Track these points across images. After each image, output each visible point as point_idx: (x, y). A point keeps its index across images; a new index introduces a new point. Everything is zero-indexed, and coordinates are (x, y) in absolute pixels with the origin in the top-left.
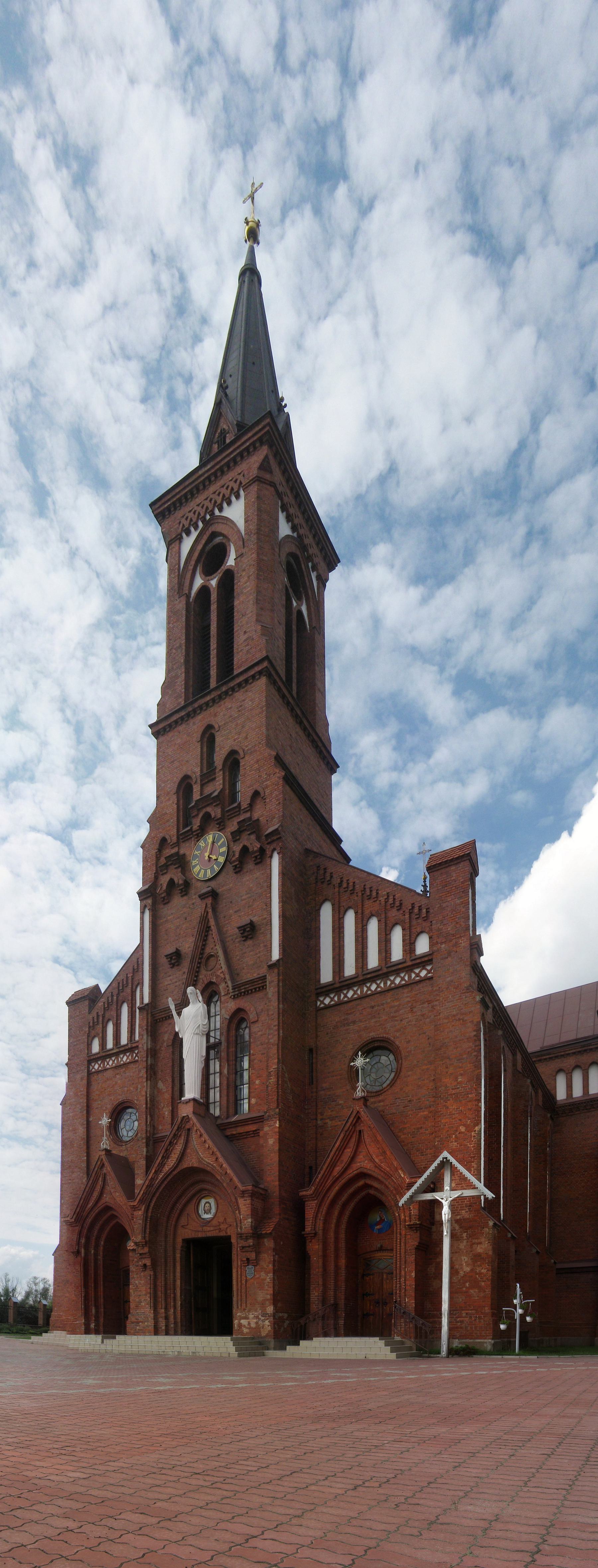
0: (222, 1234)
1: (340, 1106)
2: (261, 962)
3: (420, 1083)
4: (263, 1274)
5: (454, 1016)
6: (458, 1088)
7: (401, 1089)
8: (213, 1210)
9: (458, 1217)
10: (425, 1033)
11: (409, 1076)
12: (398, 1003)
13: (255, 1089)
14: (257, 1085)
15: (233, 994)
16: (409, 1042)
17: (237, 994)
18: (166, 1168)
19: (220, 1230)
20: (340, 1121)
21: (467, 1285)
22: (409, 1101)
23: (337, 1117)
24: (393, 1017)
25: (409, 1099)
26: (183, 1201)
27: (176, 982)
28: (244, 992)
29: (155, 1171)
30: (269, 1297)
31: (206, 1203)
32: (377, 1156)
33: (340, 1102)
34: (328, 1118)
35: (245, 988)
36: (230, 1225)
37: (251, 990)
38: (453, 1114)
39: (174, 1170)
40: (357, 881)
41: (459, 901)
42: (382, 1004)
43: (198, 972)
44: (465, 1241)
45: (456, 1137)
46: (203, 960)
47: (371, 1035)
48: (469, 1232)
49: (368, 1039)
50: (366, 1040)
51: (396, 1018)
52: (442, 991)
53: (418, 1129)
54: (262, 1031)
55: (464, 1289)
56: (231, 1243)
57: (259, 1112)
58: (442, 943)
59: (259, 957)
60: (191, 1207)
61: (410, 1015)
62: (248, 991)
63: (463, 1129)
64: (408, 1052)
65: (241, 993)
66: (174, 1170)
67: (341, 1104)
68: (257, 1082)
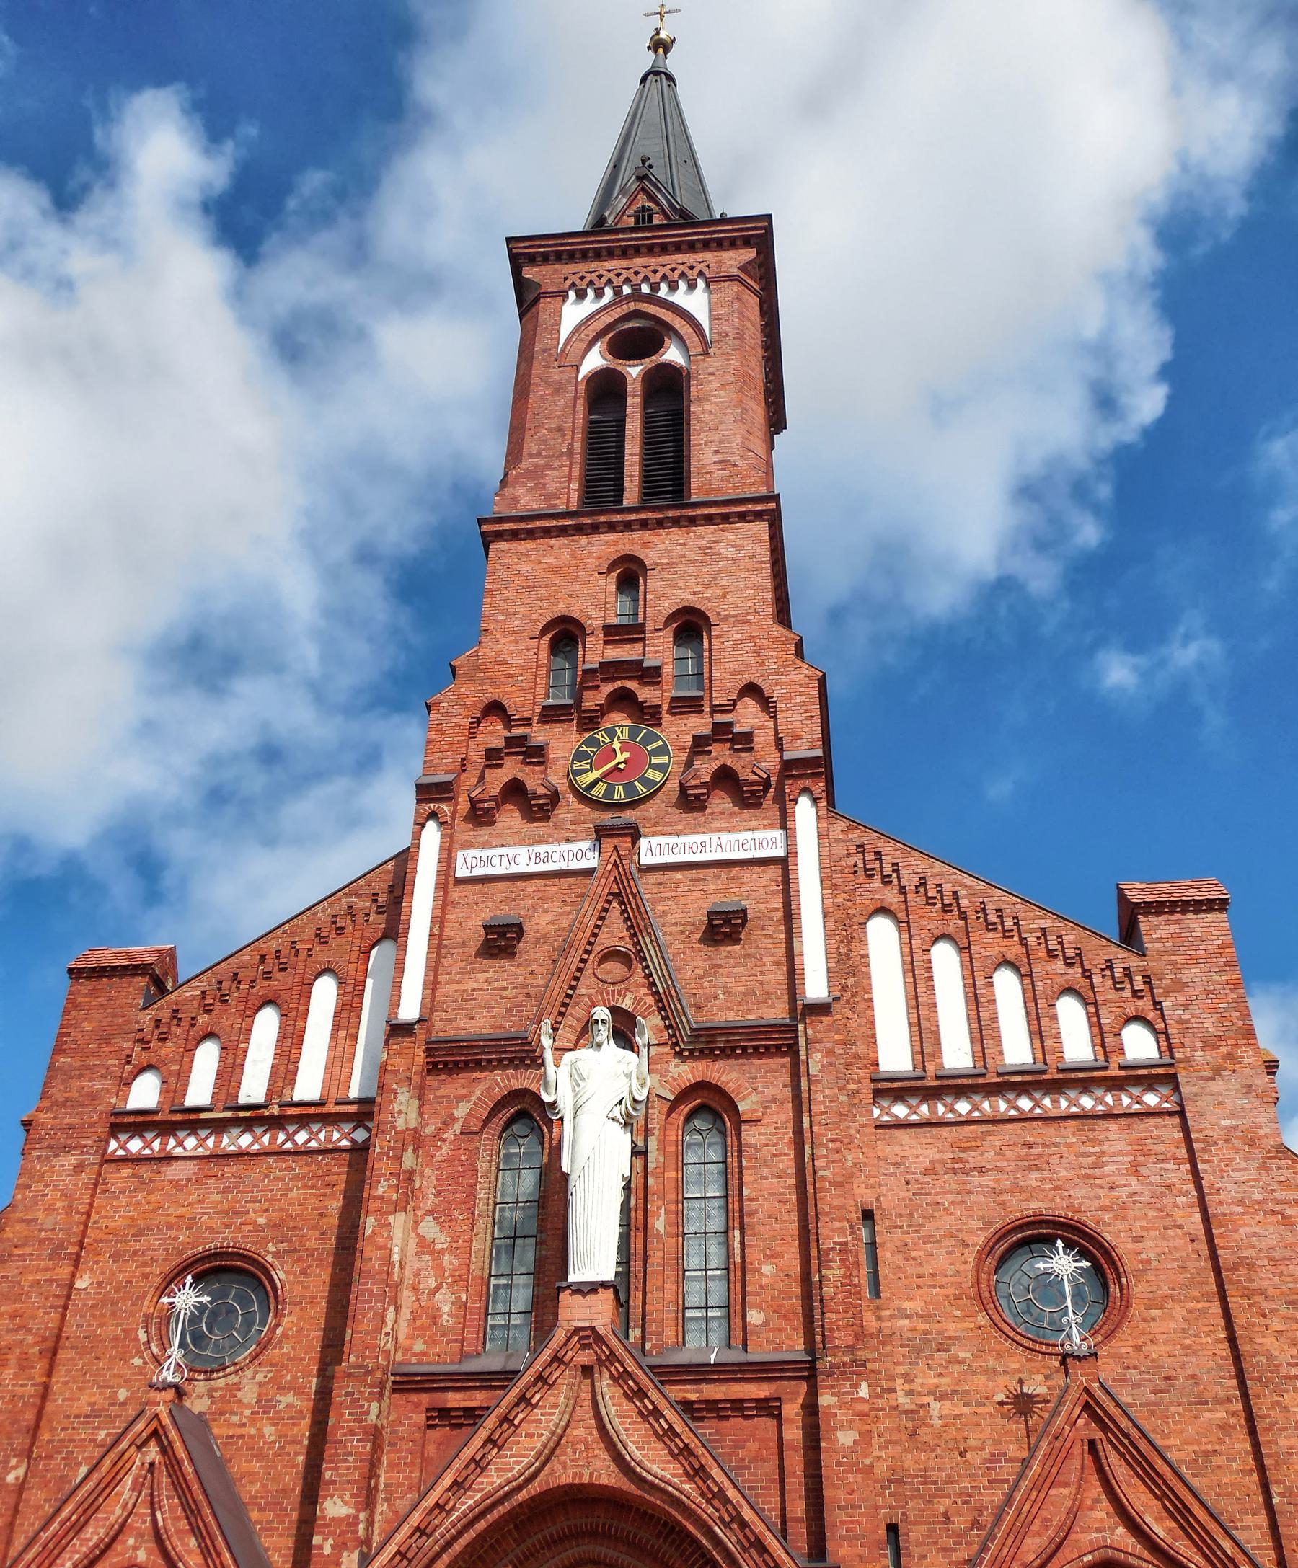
1: (963, 1367)
2: (768, 993)
3: (1188, 1342)
7: (1138, 1349)
10: (1180, 1227)
11: (1153, 1319)
12: (1096, 1149)
13: (761, 1287)
14: (767, 1276)
16: (1138, 1239)
17: (701, 1051)
18: (493, 1480)
20: (966, 1405)
22: (1168, 1378)
23: (956, 1392)
24: (1088, 1176)
25: (1164, 1372)
27: (505, 989)
28: (722, 1050)
29: (455, 1483)
33: (962, 1355)
34: (930, 1393)
35: (727, 1041)
39: (519, 1488)
40: (962, 892)
41: (1218, 978)
42: (1056, 1145)
43: (577, 979)
47: (1032, 1205)
49: (1025, 1213)
50: (1018, 1215)
51: (1097, 1181)
52: (1216, 1144)
53: (1206, 1453)
54: (776, 1145)
57: (776, 1349)
58: (1194, 1048)
59: (761, 983)
61: (1133, 1180)
62: (733, 1049)
64: (1141, 1262)
65: (712, 1050)
66: (519, 1488)
67: (964, 1361)
68: (767, 1269)
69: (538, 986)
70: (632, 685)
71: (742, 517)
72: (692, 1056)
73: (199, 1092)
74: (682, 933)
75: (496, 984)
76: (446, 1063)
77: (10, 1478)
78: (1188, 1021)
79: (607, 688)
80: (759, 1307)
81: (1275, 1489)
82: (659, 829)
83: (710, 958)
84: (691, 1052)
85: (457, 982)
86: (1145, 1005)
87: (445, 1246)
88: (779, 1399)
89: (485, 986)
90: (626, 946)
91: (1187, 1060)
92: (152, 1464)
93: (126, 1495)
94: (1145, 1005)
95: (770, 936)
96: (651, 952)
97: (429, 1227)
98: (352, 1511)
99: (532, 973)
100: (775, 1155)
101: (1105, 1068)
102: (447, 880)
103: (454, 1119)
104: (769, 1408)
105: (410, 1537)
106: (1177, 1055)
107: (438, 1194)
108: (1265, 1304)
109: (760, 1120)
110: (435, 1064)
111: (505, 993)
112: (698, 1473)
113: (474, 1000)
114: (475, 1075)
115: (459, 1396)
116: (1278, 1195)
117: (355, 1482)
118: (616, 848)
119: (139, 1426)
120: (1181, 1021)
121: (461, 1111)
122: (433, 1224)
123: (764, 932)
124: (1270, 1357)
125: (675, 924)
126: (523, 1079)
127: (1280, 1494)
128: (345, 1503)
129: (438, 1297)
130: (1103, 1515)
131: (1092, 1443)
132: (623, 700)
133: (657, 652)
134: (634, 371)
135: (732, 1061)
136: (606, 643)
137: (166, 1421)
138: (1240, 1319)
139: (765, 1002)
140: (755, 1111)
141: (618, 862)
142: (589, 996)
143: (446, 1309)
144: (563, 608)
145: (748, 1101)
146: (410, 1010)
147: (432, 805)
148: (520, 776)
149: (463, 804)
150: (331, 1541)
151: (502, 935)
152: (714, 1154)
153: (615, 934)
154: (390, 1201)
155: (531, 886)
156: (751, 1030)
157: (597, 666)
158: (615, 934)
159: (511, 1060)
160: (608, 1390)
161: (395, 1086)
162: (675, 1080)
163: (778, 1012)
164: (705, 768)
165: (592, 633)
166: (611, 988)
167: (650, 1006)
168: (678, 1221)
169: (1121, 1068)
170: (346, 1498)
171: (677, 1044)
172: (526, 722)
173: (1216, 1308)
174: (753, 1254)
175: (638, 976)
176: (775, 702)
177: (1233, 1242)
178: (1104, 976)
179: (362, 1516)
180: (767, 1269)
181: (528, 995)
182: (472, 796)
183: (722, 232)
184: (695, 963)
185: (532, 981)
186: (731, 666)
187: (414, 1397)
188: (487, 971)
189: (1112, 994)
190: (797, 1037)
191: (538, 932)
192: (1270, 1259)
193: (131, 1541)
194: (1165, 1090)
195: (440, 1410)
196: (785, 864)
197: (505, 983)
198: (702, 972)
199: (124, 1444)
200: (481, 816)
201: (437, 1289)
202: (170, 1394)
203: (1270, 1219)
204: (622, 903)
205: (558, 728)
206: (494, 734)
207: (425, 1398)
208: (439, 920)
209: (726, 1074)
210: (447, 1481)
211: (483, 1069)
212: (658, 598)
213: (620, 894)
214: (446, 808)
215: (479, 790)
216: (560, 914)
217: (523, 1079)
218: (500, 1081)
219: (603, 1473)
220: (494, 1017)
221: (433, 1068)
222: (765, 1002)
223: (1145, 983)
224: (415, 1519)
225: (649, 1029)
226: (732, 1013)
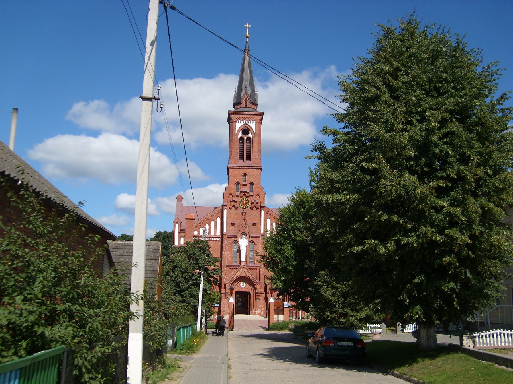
18: (237, 276)
70: (246, 193)
71: (258, 169)
73: (201, 233)
90: (245, 225)
97: (228, 252)
112: (252, 276)
121: (230, 242)
132: (244, 195)
134: (245, 137)
149: (228, 207)
153: (244, 224)
158: (244, 224)
160: (245, 269)
164: (253, 205)
183: (257, 113)
209: (254, 240)
218: (234, 239)
219: (245, 275)
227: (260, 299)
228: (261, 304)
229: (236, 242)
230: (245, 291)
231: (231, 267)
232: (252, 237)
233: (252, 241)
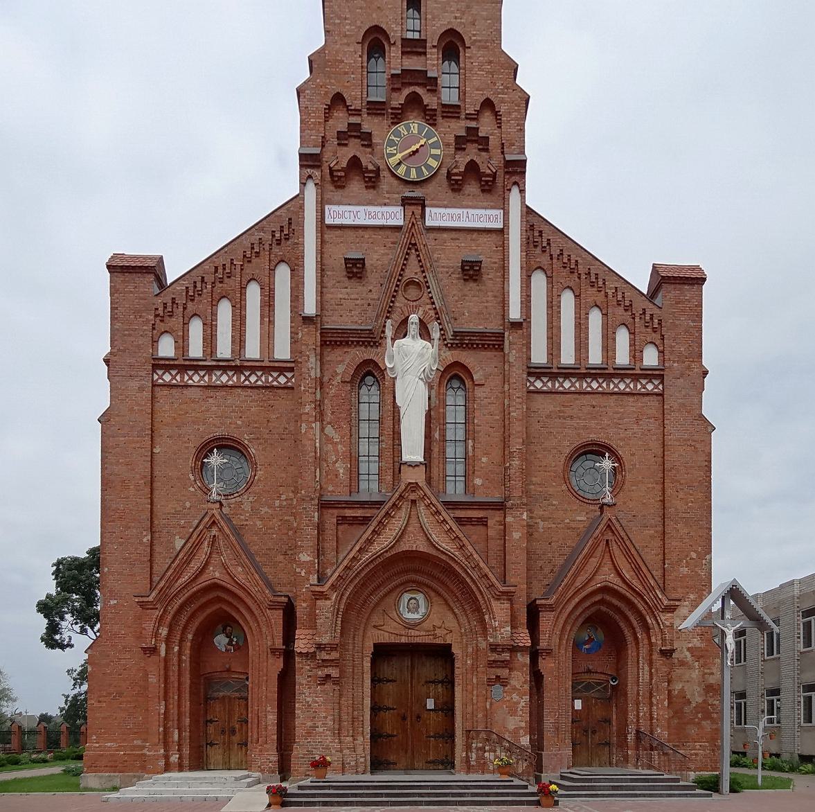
0: (438, 641)
2: (490, 314)
4: (515, 697)
5: (685, 440)
6: (689, 513)
8: (422, 610)
9: (690, 645)
13: (481, 468)
15: (452, 342)
19: (435, 636)
21: (700, 715)
26: (383, 591)
28: (467, 344)
30: (523, 724)
31: (411, 599)
32: (628, 572)
36: (451, 631)
37: (478, 345)
38: (685, 539)
41: (692, 324)
44: (697, 671)
45: (687, 561)
46: (402, 285)
48: (702, 661)
55: (696, 720)
56: (453, 654)
58: (674, 362)
60: (390, 600)
63: (694, 555)
68: (484, 459)
69: (374, 299)
72: (451, 347)
74: (447, 273)
75: (353, 297)
76: (330, 341)
77: (145, 540)
78: (674, 347)
79: (406, 92)
80: (480, 477)
81: (666, 562)
82: (435, 202)
83: (461, 290)
84: (452, 344)
85: (332, 293)
86: (657, 336)
87: (338, 440)
88: (487, 518)
89: (346, 297)
91: (670, 367)
92: (214, 536)
93: (206, 549)
94: (657, 336)
95: (491, 279)
96: (432, 283)
97: (329, 430)
98: (312, 559)
99: (371, 291)
100: (489, 403)
101: (634, 369)
102: (323, 228)
103: (337, 374)
104: (483, 522)
105: (343, 570)
106: (666, 365)
107: (333, 413)
108: (679, 487)
109: (483, 385)
110: (325, 341)
111: (358, 302)
113: (342, 305)
114: (345, 350)
115: (350, 511)
116: (695, 438)
117: (311, 546)
118: (413, 213)
119: (206, 519)
120: (671, 347)
121: (340, 369)
122: (331, 428)
123: (489, 277)
124: (676, 509)
125: (443, 267)
126: (369, 354)
127: (669, 564)
128: (309, 555)
129: (337, 465)
130: (607, 569)
131: (607, 541)
133: (434, 65)
135: (471, 352)
136: (403, 53)
137: (218, 517)
138: (668, 492)
139: (487, 319)
140: (482, 380)
141: (415, 222)
142: (401, 308)
143: (341, 471)
144: (375, 19)
145: (478, 374)
146: (310, 308)
147: (309, 170)
148: (358, 154)
150: (304, 570)
151: (354, 265)
152: (461, 401)
154: (312, 416)
155: (367, 235)
156: (482, 335)
157: (400, 72)
159: (363, 342)
161: (307, 353)
162: (444, 360)
163: (493, 326)
165: (395, 43)
166: (411, 304)
167: (432, 316)
168: (443, 435)
169: (642, 369)
170: (309, 553)
171: (445, 340)
172: (357, 112)
173: (659, 487)
174: (478, 452)
175: (425, 299)
176: (501, 115)
177: (672, 458)
178: (640, 318)
179: (316, 561)
180: (484, 459)
181: (369, 305)
182: (332, 166)
184: (454, 293)
185: (370, 296)
186: (477, 84)
187: (330, 511)
188: (346, 288)
189: (643, 329)
190: (503, 341)
191: (372, 265)
192: (685, 467)
193: (211, 568)
194: (656, 382)
195: (342, 517)
196: (502, 232)
197: (357, 296)
198: (457, 298)
199: (201, 527)
200: (336, 181)
201: (336, 462)
202: (218, 505)
203: (689, 448)
204: (417, 250)
205: (376, 120)
206: (341, 121)
207: (336, 512)
208: (321, 252)
209: (467, 358)
210: (357, 548)
211: (349, 346)
212: (433, 19)
213: (415, 244)
214: (317, 173)
215: (335, 162)
216: (383, 254)
217: (369, 354)
220: (352, 316)
221: (324, 344)
222: (487, 319)
223: (659, 324)
224: (345, 563)
225: (436, 335)
226: (472, 324)
227: (513, 682)
228: (513, 711)
229: (371, 372)
230: (428, 640)
231: (349, 513)
232: (461, 341)
233: (457, 364)
